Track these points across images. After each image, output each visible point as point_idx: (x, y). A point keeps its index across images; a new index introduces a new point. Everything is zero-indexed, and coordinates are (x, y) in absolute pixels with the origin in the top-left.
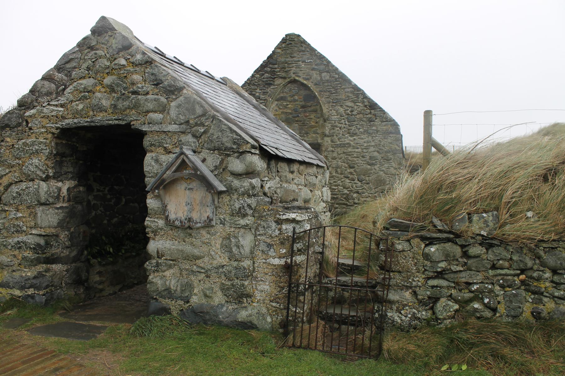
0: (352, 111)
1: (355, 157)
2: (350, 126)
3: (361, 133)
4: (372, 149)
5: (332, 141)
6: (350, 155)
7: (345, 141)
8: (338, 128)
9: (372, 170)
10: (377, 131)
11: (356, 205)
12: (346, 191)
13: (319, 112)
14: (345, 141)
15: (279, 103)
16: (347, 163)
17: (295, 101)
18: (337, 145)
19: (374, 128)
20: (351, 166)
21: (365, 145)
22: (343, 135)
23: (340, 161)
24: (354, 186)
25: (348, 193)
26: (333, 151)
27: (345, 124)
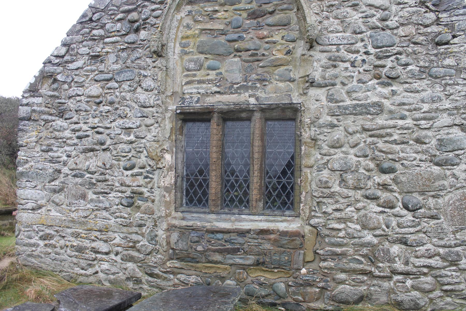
0: (384, 20)
1: (395, 142)
2: (379, 58)
3: (413, 76)
4: (445, 119)
5: (331, 99)
6: (381, 136)
7: (367, 98)
8: (348, 65)
9: (445, 177)
11: (396, 278)
12: (369, 237)
13: (294, 25)
14: (367, 98)
15: (196, 7)
16: (373, 159)
18: (346, 108)
19: (449, 61)
20: (386, 165)
21: (426, 107)
22: (360, 81)
23: (352, 151)
24: (394, 224)
25: (375, 241)
26: (333, 126)
27: (367, 53)
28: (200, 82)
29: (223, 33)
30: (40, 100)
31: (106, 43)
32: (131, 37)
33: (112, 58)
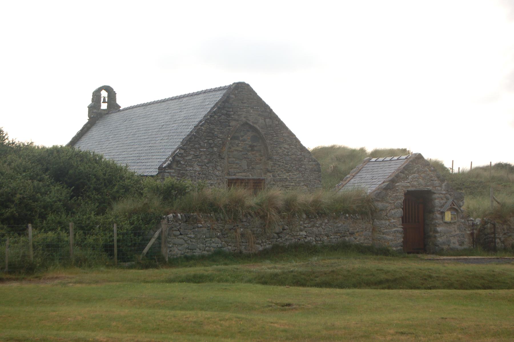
5: (274, 176)
10: (306, 169)
17: (244, 141)
28: (235, 168)
29: (241, 151)
30: (173, 171)
31: (201, 151)
32: (210, 150)
33: (204, 157)
